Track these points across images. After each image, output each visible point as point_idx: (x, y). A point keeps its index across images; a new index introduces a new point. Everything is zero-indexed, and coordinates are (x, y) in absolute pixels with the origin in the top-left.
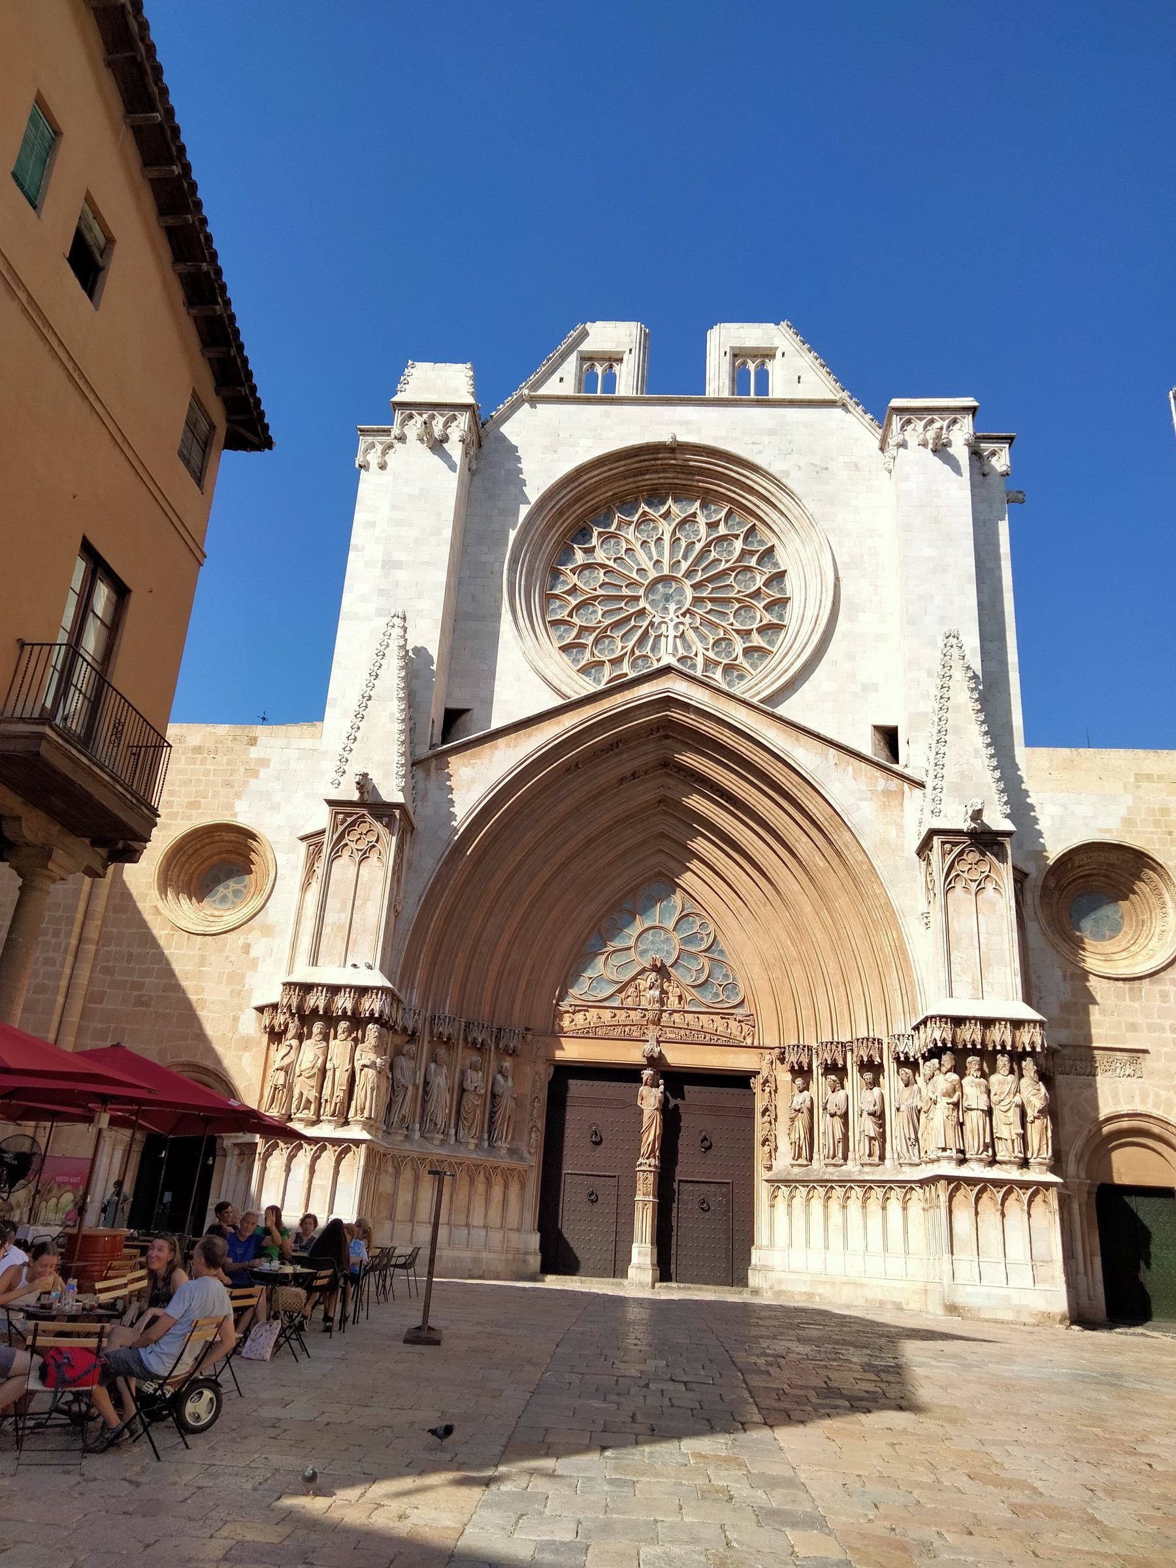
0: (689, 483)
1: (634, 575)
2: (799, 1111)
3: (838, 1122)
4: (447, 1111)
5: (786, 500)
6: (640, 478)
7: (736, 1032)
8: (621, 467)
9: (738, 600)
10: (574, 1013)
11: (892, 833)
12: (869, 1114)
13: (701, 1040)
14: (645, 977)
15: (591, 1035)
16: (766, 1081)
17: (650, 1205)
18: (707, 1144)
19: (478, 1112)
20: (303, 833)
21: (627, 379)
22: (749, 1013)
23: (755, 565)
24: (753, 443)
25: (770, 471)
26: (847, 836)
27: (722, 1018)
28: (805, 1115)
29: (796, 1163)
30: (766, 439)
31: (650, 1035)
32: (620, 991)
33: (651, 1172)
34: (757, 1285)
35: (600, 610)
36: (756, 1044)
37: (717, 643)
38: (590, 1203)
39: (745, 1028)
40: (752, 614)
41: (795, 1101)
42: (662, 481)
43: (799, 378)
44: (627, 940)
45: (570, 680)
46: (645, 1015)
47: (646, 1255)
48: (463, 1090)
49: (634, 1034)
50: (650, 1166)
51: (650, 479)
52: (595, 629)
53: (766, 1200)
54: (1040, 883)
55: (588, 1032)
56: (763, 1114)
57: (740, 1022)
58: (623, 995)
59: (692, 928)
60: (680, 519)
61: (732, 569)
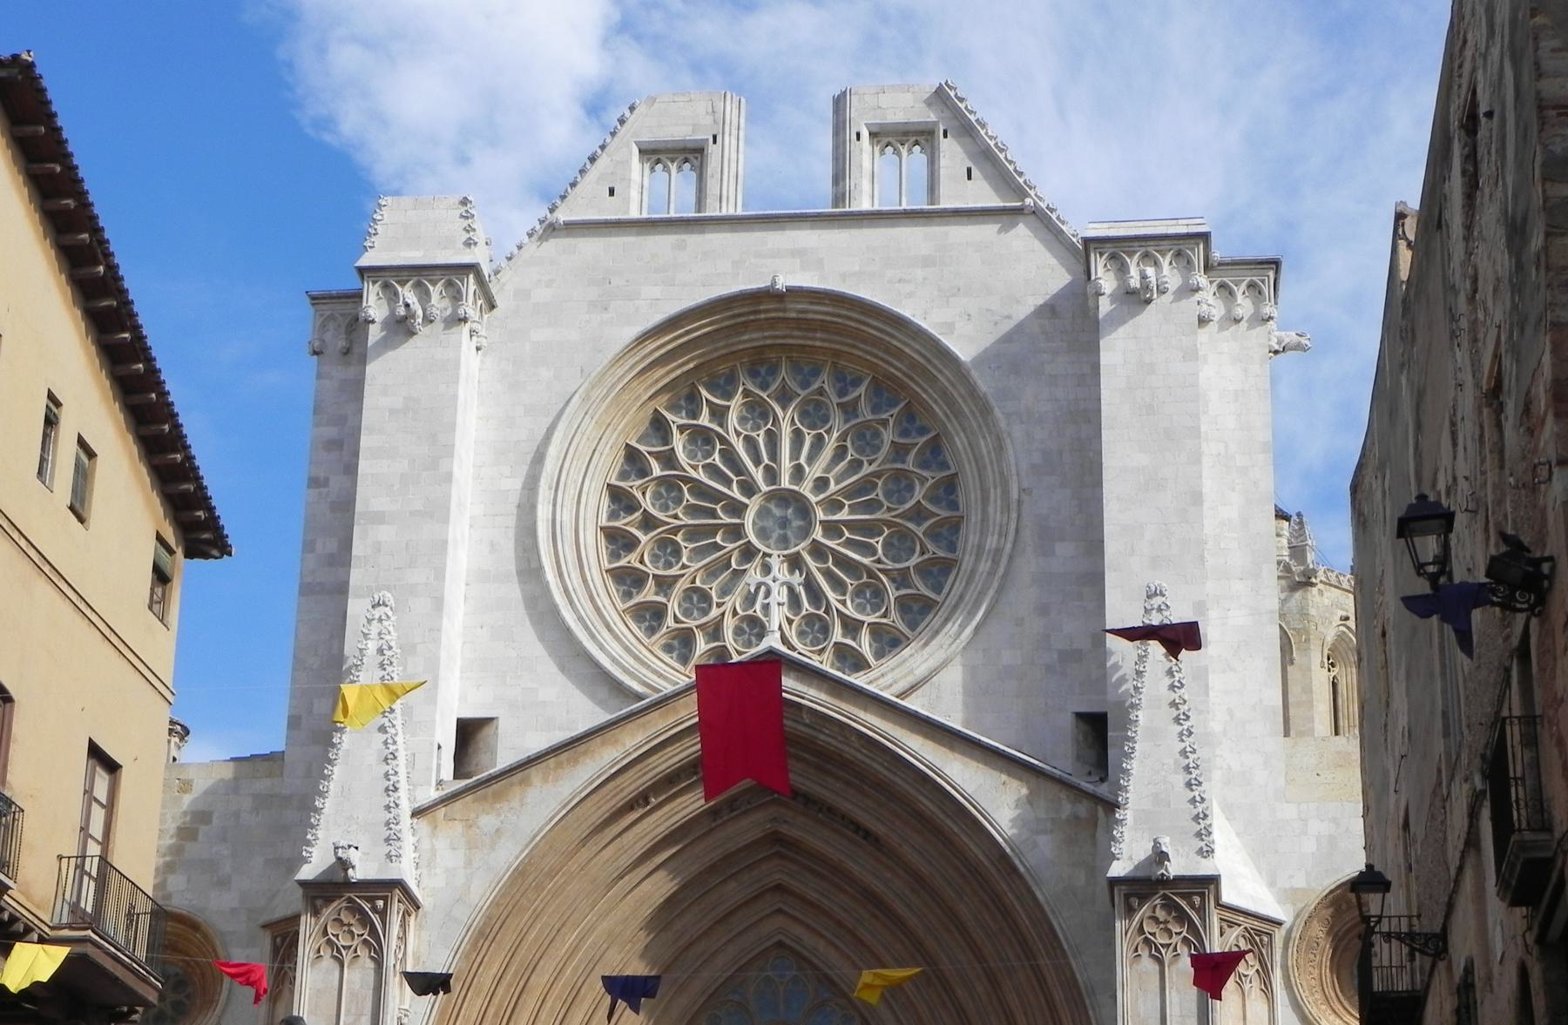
0: (809, 343)
1: (736, 493)
8: (702, 328)
9: (889, 524)
11: (1081, 878)
20: (265, 918)
23: (911, 468)
24: (900, 281)
25: (924, 325)
30: (919, 273)
35: (687, 547)
37: (858, 592)
40: (909, 544)
42: (769, 342)
43: (969, 171)
45: (637, 666)
51: (751, 339)
52: (677, 578)
54: (1296, 934)
60: (800, 398)
61: (877, 474)
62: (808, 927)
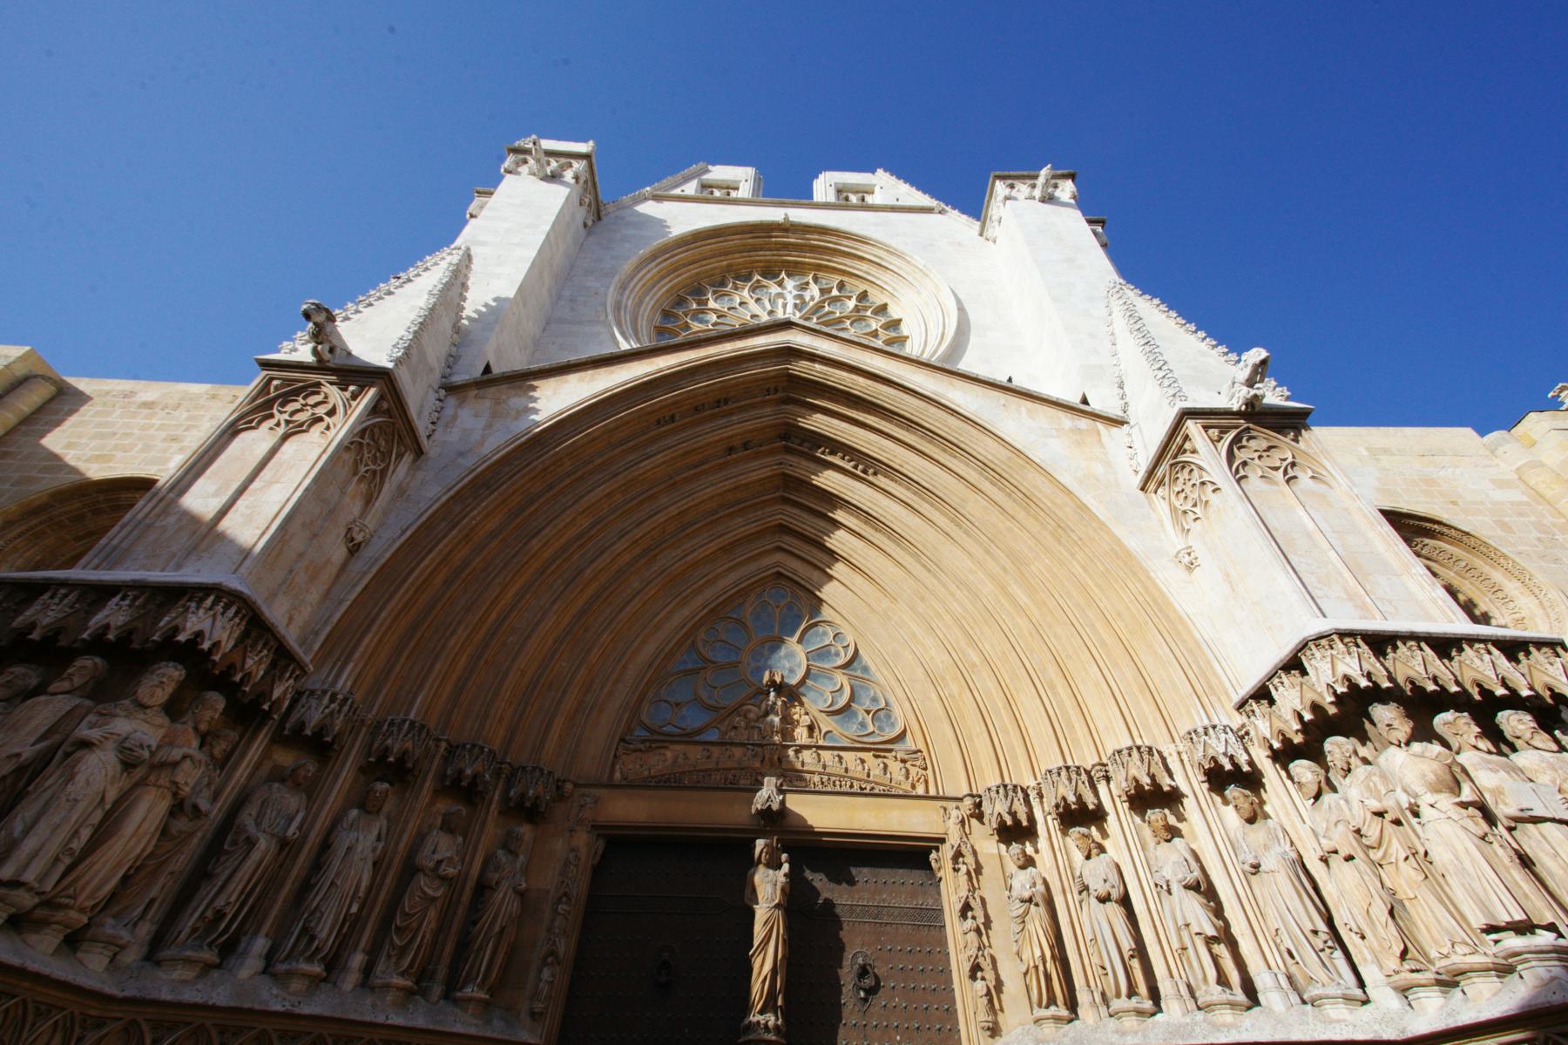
2: (1030, 900)
3: (1115, 912)
4: (354, 909)
5: (898, 262)
6: (754, 253)
12: (1187, 887)
13: (846, 789)
16: (958, 855)
18: (868, 982)
19: (432, 914)
21: (745, 191)
22: (914, 748)
26: (1039, 480)
27: (876, 757)
28: (1038, 914)
36: (932, 792)
48: (410, 869)
49: (742, 782)
51: (766, 255)
57: (903, 761)
62: (803, 559)
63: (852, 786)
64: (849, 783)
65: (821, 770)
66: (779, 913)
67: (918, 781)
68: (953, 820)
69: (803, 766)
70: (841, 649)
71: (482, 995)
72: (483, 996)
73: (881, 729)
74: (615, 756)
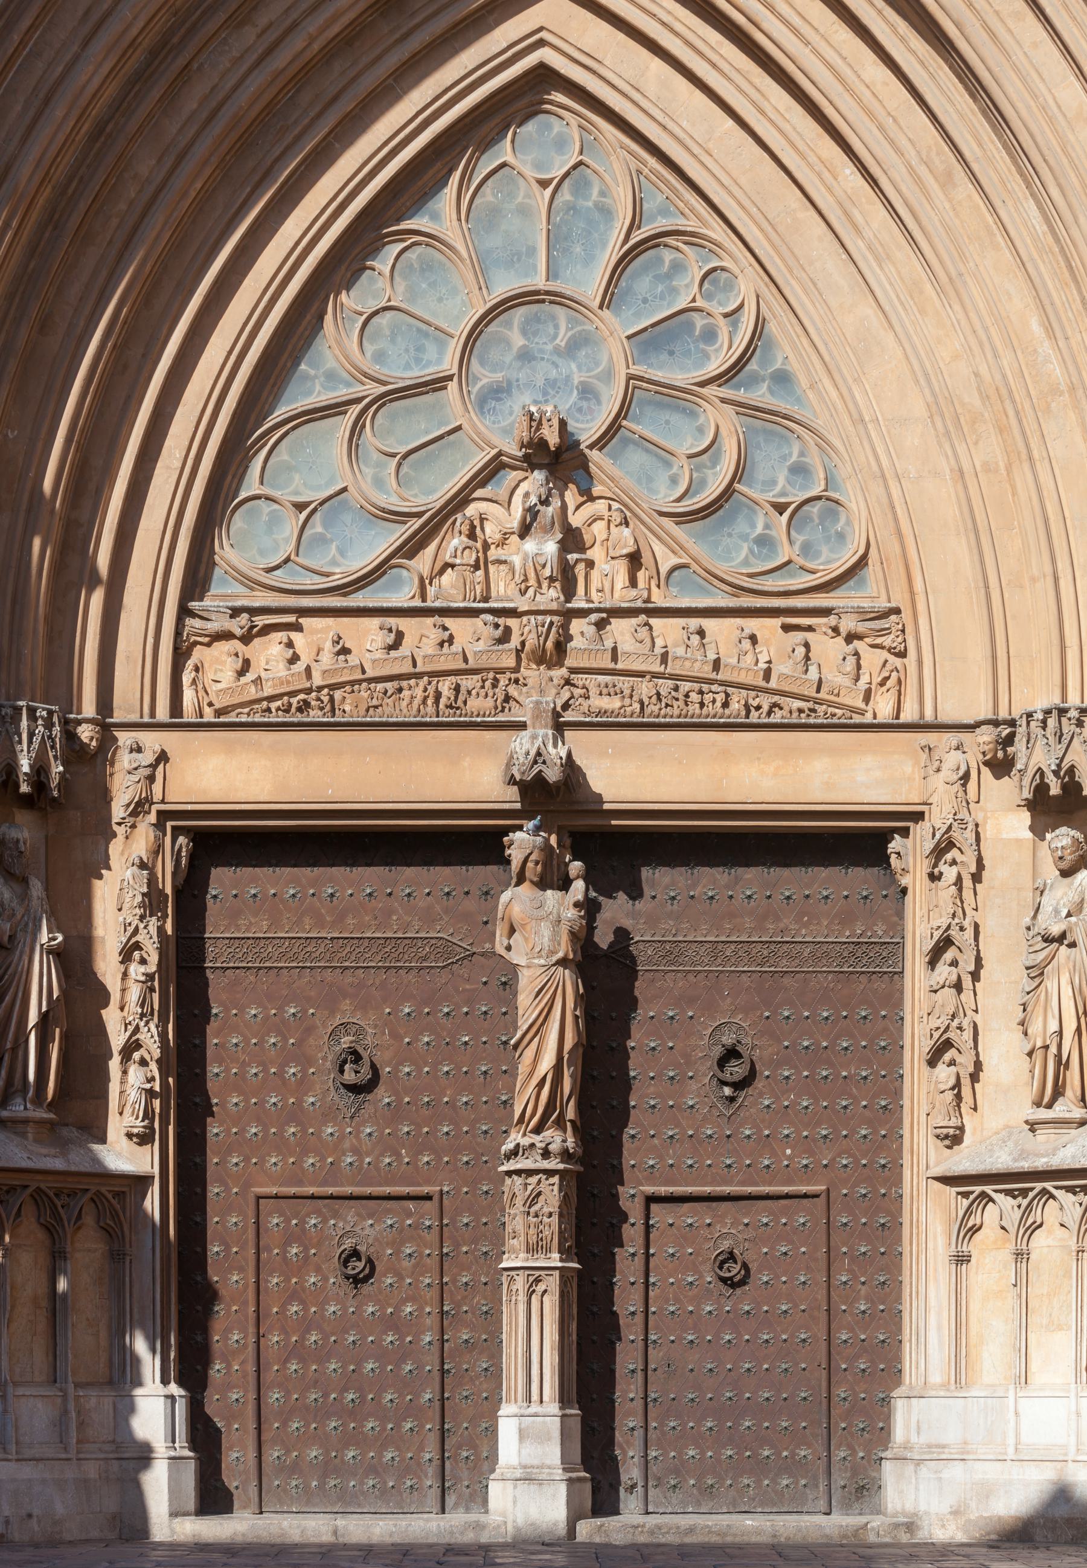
2: (1061, 938)
7: (836, 678)
10: (246, 639)
13: (713, 710)
14: (502, 493)
15: (315, 715)
16: (943, 848)
17: (552, 1282)
22: (883, 604)
27: (787, 628)
29: (1043, 1114)
31: (528, 702)
32: (411, 548)
33: (550, 1173)
34: (909, 1507)
36: (909, 715)
38: (347, 1287)
39: (872, 659)
41: (1047, 906)
44: (431, 350)
46: (508, 631)
47: (542, 1438)
49: (474, 704)
50: (546, 1154)
53: (941, 1241)
55: (304, 707)
56: (934, 957)
57: (850, 638)
58: (423, 562)
59: (674, 291)
63: (726, 705)
64: (720, 698)
65: (658, 668)
66: (567, 975)
67: (882, 684)
68: (948, 773)
69: (615, 658)
70: (722, 322)
71: (42, 1114)
72: (45, 1115)
73: (807, 549)
74: (176, 649)
